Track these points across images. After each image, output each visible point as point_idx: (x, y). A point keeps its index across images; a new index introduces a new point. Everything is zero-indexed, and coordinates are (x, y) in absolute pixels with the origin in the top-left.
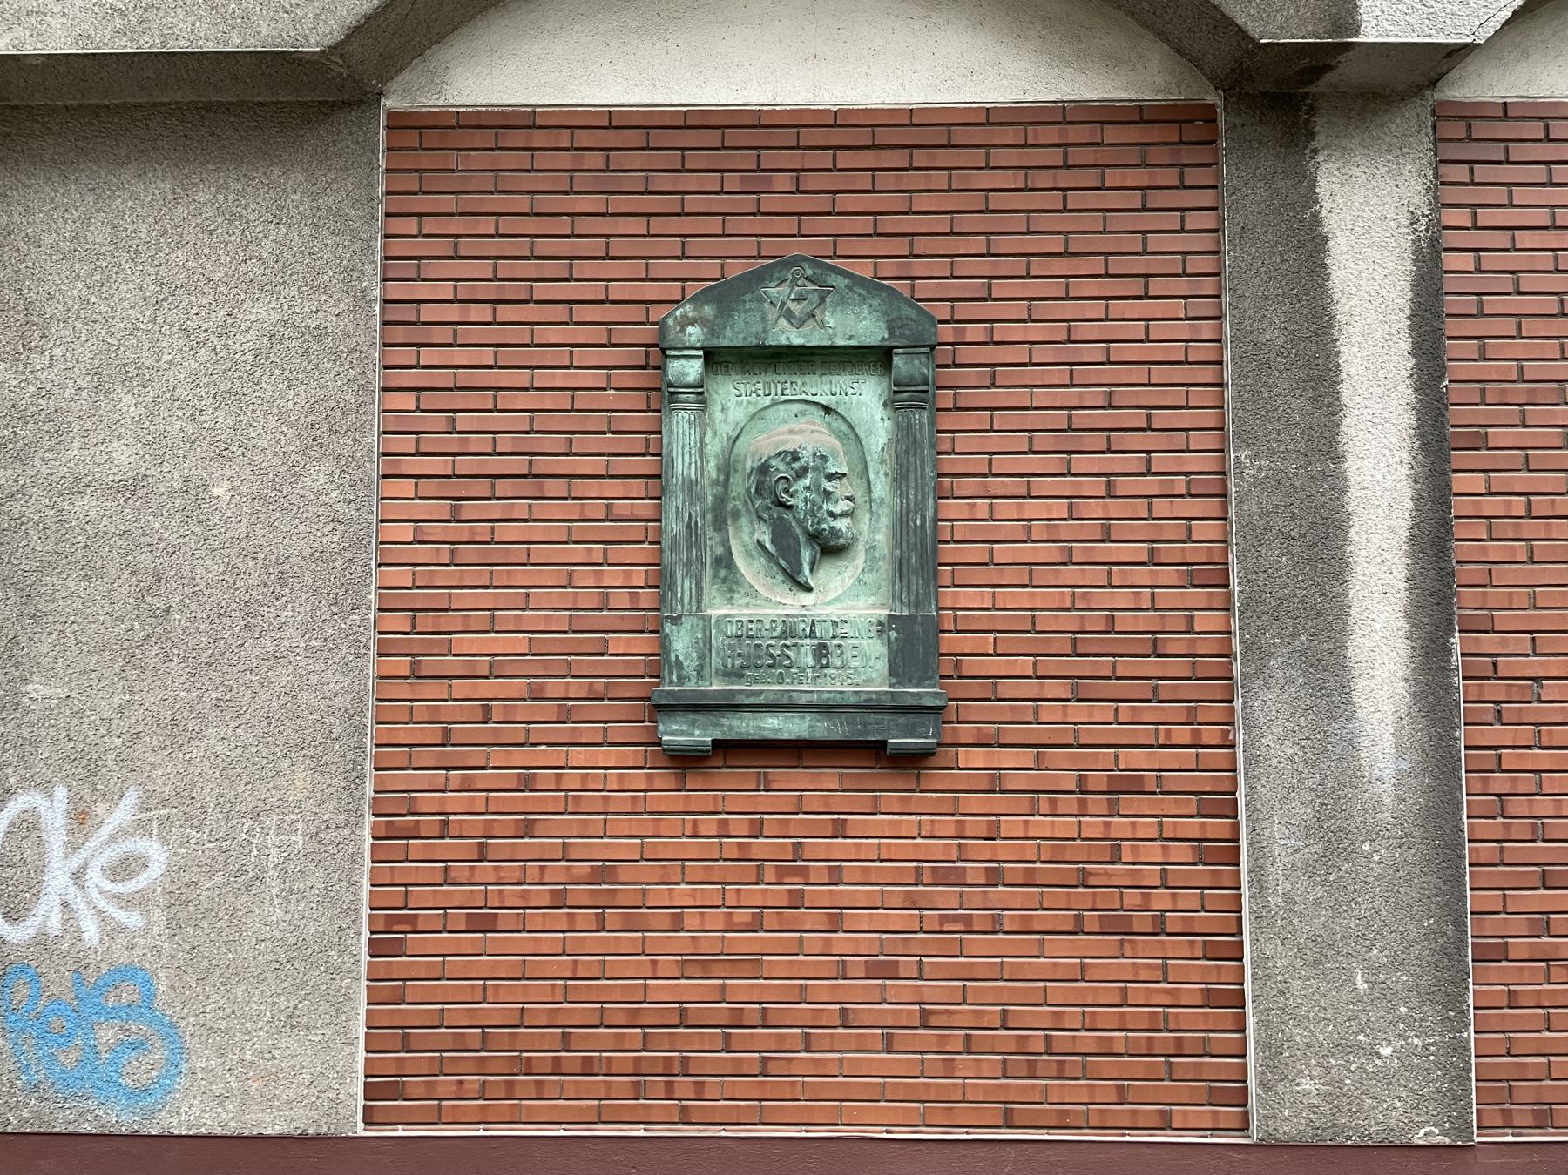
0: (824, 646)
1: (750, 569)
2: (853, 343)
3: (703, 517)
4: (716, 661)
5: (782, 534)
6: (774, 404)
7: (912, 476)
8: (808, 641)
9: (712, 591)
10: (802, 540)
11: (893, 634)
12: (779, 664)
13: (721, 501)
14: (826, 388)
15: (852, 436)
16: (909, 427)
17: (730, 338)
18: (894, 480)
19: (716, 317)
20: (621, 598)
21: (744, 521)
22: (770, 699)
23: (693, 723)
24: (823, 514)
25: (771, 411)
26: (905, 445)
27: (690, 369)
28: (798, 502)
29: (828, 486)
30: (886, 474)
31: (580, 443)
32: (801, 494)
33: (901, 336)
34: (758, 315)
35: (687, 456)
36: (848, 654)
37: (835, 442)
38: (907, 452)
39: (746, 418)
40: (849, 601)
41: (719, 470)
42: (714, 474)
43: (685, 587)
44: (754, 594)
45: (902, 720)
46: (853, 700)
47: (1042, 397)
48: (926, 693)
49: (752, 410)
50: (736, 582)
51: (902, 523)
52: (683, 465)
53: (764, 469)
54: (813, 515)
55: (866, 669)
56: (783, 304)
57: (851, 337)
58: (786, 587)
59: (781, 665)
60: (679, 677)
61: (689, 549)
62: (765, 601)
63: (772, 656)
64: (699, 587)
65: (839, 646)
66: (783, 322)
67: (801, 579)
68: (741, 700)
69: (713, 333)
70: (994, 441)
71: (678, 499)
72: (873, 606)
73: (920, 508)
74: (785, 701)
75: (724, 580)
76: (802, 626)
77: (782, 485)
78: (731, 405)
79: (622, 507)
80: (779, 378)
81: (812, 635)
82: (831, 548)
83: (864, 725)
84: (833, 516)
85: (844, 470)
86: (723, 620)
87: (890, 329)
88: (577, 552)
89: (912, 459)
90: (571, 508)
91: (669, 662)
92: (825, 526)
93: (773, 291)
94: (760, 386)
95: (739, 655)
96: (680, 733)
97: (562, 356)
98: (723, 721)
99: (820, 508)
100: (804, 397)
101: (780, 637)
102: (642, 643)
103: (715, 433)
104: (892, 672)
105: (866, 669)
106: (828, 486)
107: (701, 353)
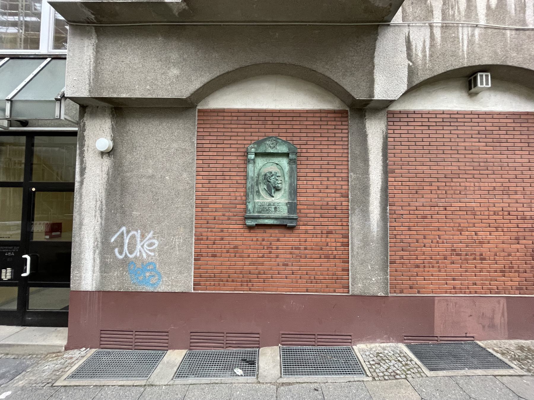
1: (263, 193)
4: (256, 210)
5: (268, 187)
9: (256, 197)
12: (268, 211)
13: (257, 181)
15: (282, 169)
20: (239, 198)
26: (291, 171)
27: (252, 156)
28: (272, 181)
32: (272, 180)
37: (279, 170)
40: (281, 199)
43: (251, 196)
44: (263, 198)
47: (316, 162)
48: (294, 216)
51: (290, 185)
52: (251, 174)
53: (265, 175)
55: (284, 212)
69: (256, 150)
70: (307, 170)
71: (250, 180)
73: (294, 183)
78: (260, 162)
79: (239, 181)
82: (277, 189)
86: (258, 202)
88: (231, 190)
90: (230, 182)
96: (249, 223)
102: (243, 206)
104: (288, 212)
105: (284, 212)
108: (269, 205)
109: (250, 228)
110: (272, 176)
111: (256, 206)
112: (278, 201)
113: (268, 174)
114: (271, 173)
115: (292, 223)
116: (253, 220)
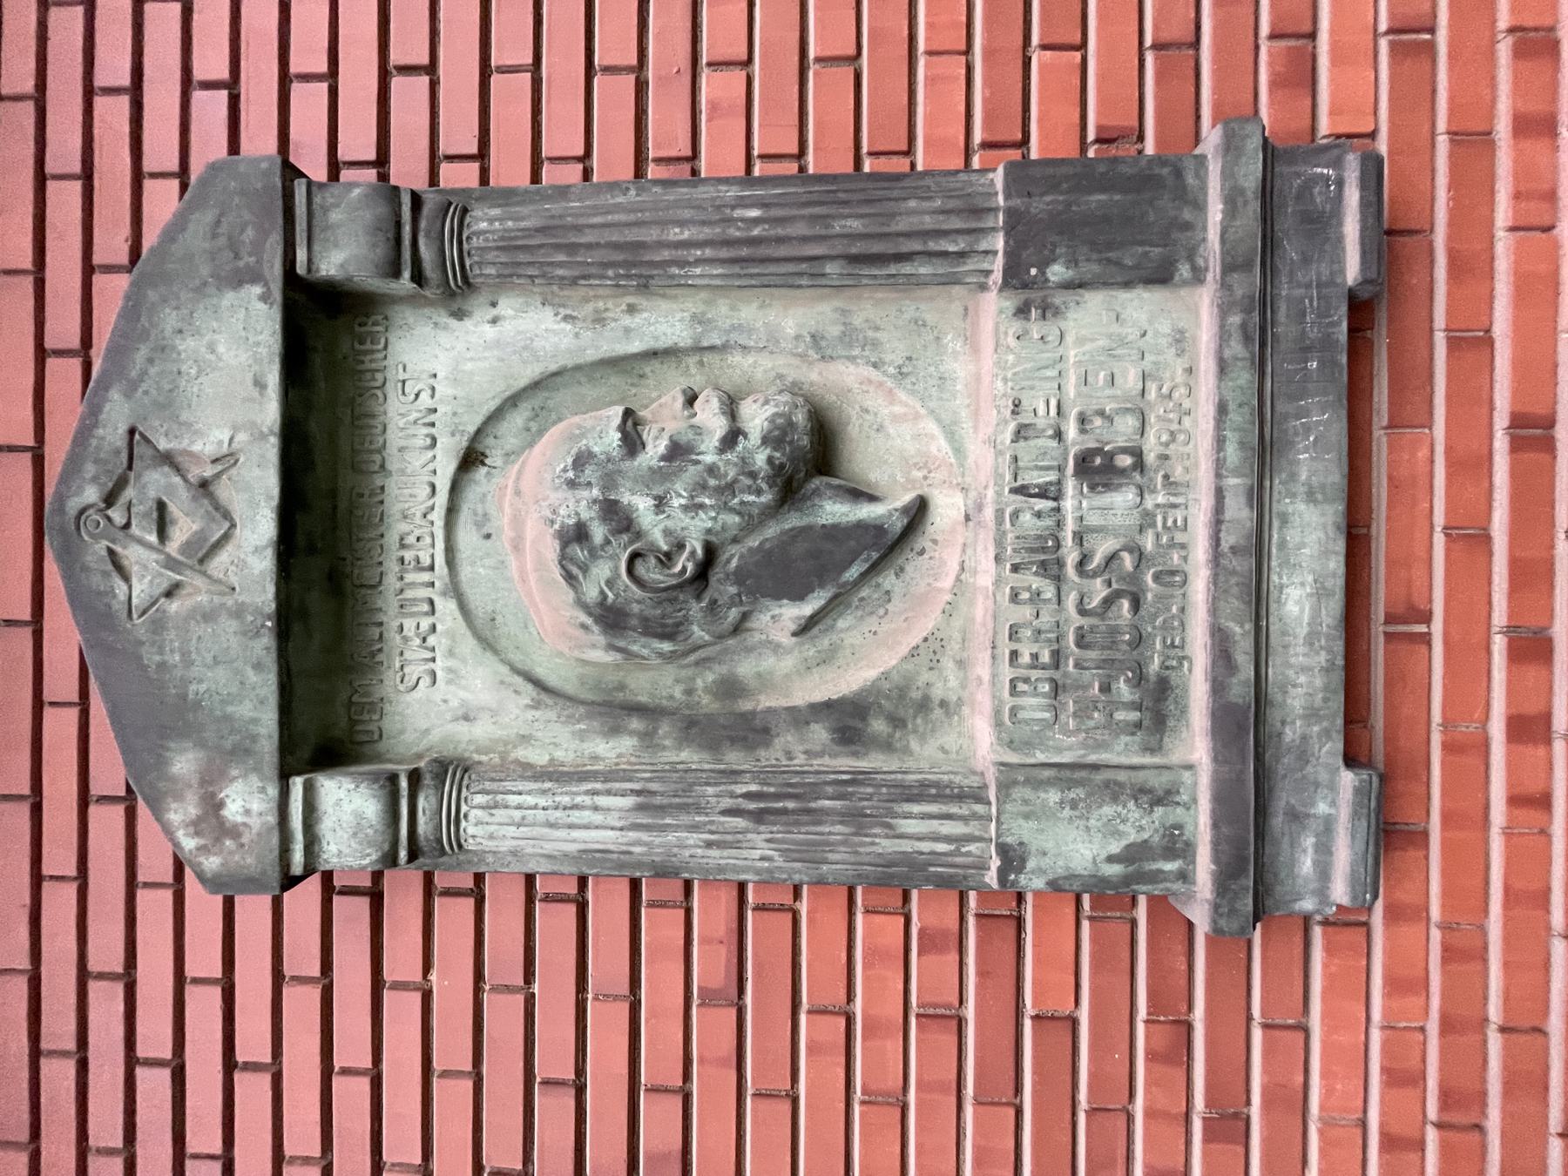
0: (1084, 465)
1: (865, 656)
2: (273, 378)
3: (733, 775)
4: (1123, 752)
5: (780, 575)
6: (455, 591)
7: (632, 235)
8: (1068, 504)
9: (926, 755)
10: (793, 521)
11: (1057, 272)
12: (1135, 581)
13: (694, 728)
14: (416, 461)
15: (538, 394)
16: (508, 245)
17: (257, 707)
18: (644, 287)
19: (201, 744)
20: (929, 976)
21: (746, 668)
22: (1234, 604)
23: (1296, 817)
24: (728, 465)
25: (479, 600)
26: (562, 259)
27: (347, 808)
28: (695, 530)
29: (655, 449)
31: (554, 1060)
32: (677, 521)
34: (198, 629)
35: (576, 816)
37: (555, 432)
38: (572, 248)
40: (952, 399)
41: (614, 731)
43: (918, 831)
44: (931, 649)
45: (1291, 251)
46: (1244, 377)
49: (468, 644)
50: (902, 692)
51: (757, 262)
52: (599, 826)
53: (610, 618)
54: (730, 488)
57: (260, 384)
58: (915, 566)
59: (1135, 577)
61: (817, 816)
63: (1108, 602)
65: (1083, 420)
67: (898, 524)
69: (242, 752)
71: (685, 843)
73: (721, 213)
74: (1245, 565)
75: (897, 722)
76: (1026, 518)
77: (649, 570)
78: (456, 697)
79: (710, 966)
80: (391, 582)
81: (1050, 492)
82: (814, 452)
83: (1305, 351)
86: (1008, 727)
87: (239, 279)
89: (588, 237)
90: (711, 1089)
91: (1127, 880)
93: (141, 589)
94: (409, 625)
95: (1106, 688)
97: (351, 1095)
98: (1290, 735)
100: (438, 517)
101: (1058, 579)
103: (525, 739)
106: (655, 449)
108: (1051, 569)
109: (1390, 835)
110: (617, 517)
111: (1066, 747)
113: (591, 593)
114: (579, 534)
115: (1322, 225)
116: (1283, 799)
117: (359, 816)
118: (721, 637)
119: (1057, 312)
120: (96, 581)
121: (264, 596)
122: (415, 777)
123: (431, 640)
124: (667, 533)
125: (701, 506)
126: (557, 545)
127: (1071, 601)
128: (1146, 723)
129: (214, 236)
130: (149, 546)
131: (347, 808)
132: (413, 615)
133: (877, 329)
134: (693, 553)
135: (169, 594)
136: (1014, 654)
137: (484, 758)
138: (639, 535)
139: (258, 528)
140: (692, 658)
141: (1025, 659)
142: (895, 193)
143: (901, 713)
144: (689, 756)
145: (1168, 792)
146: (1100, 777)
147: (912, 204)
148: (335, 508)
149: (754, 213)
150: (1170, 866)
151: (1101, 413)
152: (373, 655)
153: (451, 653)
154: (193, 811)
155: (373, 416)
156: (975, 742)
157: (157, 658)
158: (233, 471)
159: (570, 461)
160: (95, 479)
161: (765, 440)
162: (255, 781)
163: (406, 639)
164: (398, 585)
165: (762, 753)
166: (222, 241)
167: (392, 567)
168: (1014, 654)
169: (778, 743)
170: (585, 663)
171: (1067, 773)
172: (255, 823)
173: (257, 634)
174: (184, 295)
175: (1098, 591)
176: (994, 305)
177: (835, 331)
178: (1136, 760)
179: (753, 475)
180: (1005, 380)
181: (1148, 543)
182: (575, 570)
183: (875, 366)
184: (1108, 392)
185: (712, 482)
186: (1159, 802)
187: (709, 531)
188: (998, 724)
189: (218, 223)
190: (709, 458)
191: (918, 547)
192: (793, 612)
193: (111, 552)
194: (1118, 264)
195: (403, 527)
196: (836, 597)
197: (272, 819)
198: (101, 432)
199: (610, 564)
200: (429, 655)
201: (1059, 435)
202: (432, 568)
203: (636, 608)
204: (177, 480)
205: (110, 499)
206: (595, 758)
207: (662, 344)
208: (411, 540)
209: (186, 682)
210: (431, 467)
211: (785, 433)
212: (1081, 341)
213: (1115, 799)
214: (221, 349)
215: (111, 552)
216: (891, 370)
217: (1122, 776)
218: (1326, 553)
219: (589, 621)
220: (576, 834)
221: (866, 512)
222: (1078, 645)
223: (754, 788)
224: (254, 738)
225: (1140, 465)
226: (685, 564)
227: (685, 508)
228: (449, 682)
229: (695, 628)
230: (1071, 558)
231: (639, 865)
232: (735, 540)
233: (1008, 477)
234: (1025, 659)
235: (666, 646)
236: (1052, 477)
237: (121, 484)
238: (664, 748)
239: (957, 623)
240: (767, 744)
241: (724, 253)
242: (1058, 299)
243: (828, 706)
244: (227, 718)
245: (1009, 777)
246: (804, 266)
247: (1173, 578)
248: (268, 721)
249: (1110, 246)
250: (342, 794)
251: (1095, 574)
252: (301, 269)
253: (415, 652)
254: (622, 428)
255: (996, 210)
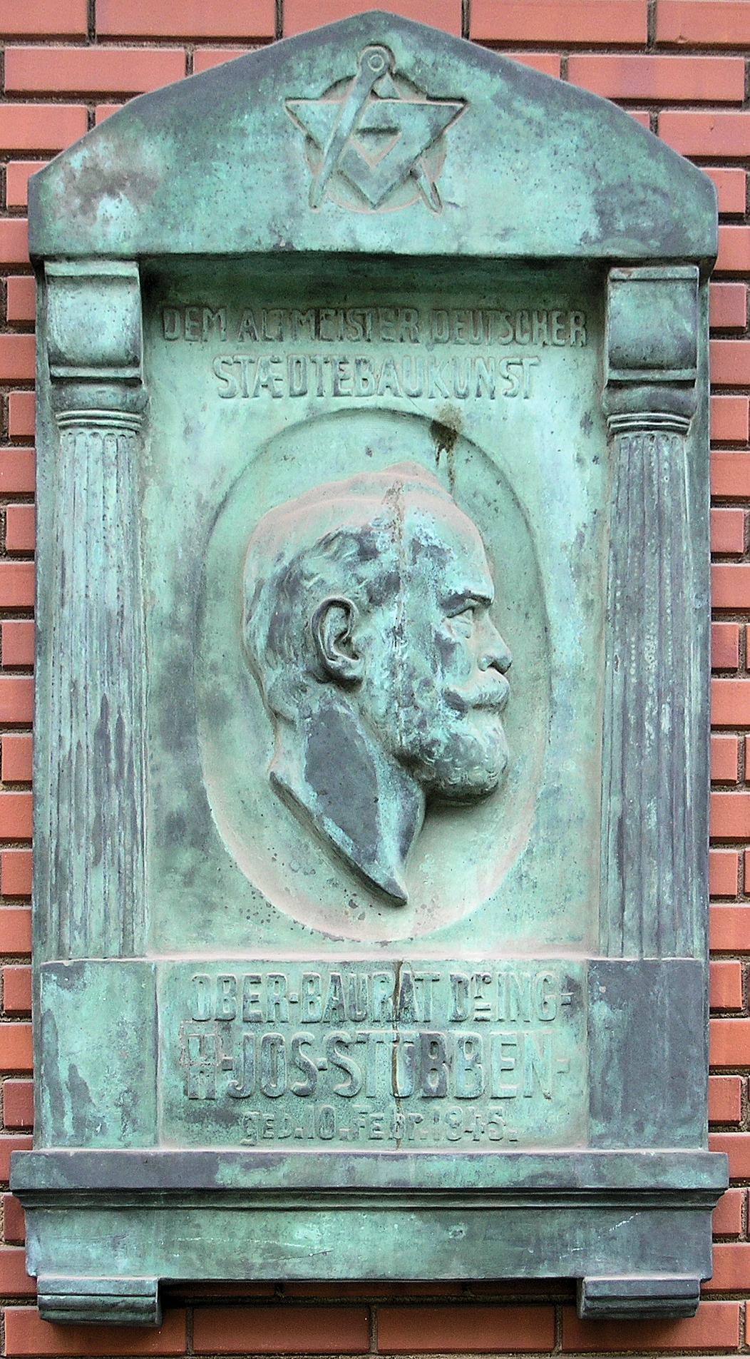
4: (169, 1082)
5: (331, 758)
6: (314, 418)
10: (383, 769)
11: (601, 1011)
13: (180, 672)
19: (170, 174)
21: (238, 726)
25: (305, 442)
28: (372, 668)
30: (588, 604)
33: (631, 232)
34: (277, 169)
36: (495, 1061)
39: (239, 453)
41: (178, 590)
42: (165, 602)
43: (92, 890)
44: (261, 913)
49: (261, 432)
50: (217, 882)
53: (289, 584)
54: (411, 702)
56: (339, 141)
57: (505, 234)
60: (79, 1123)
62: (279, 934)
63: (305, 1069)
64: (128, 895)
66: (337, 196)
67: (377, 874)
68: (228, 1176)
72: (552, 943)
74: (338, 1179)
78: (209, 420)
80: (323, 349)
82: (449, 798)
84: (457, 704)
85: (484, 588)
92: (437, 732)
93: (315, 111)
94: (279, 370)
99: (427, 683)
100: (388, 400)
103: (168, 494)
104: (598, 1108)
107: (132, 270)
108: (337, 1013)
112: (470, 955)
113: (310, 565)
114: (367, 553)
117: (100, 328)
118: (269, 699)
119: (569, 1016)
120: (324, 64)
121: (309, 239)
122: (133, 383)
123: (265, 393)
124: (369, 641)
125: (393, 674)
126: (357, 530)
127: (307, 1034)
128: (195, 1103)
129: (645, 187)
130: (355, 122)
131: (107, 317)
132: (290, 375)
133: (564, 853)
134: (350, 666)
135: (309, 139)
136: (256, 981)
137: (148, 449)
138: (366, 612)
139: (372, 233)
140: (247, 671)
141: (253, 991)
142: (680, 862)
143: (197, 881)
144: (151, 670)
145: (134, 1122)
146: (146, 1057)
147: (669, 877)
148: (397, 290)
149: (666, 725)
150: (68, 1122)
151: (476, 1060)
152: (251, 331)
153: (252, 414)
154: (108, 166)
155: (486, 332)
156: (173, 948)
157: (250, 129)
158: (425, 208)
159: (436, 543)
160: (418, 62)
161: (455, 737)
162: (136, 229)
163: (266, 367)
164: (320, 359)
165: (158, 741)
166: (641, 195)
167: (338, 349)
168: (256, 981)
169: (167, 758)
170: (243, 557)
171: (150, 1029)
172: (95, 230)
173: (272, 231)
174: (589, 157)
175: (316, 1059)
176: (575, 961)
177: (563, 812)
178: (160, 1095)
179: (422, 724)
180: (508, 969)
181: (360, 1104)
182: (335, 547)
183: (529, 852)
184: (496, 1067)
185: (415, 685)
186: (126, 1113)
187: (370, 683)
188: (193, 966)
189: (655, 190)
190: (438, 682)
191: (357, 900)
192: (295, 776)
193: (350, 78)
194: (607, 1067)
195: (377, 362)
196: (308, 813)
197: (100, 246)
198: (463, 67)
199: (340, 584)
200: (250, 392)
201: (457, 1021)
202: (337, 394)
203: (298, 609)
204: (417, 150)
205: (400, 76)
206: (149, 568)
207: (554, 634)
208: (365, 372)
209: (227, 156)
210: (438, 394)
211: (462, 757)
212: (541, 1041)
213: (128, 1073)
214: (539, 194)
215: (350, 78)
216: (525, 868)
217: (148, 1078)
218: (348, 1261)
219: (286, 562)
220: (81, 550)
221: (389, 845)
222: (266, 1039)
223: (127, 730)
224: (174, 228)
225: (428, 1098)
226: (339, 660)
227: (392, 658)
228: (223, 412)
229: (279, 671)
230: (345, 1034)
231: (48, 615)
232: (362, 711)
233: (419, 974)
234: (253, 991)
235: (261, 642)
236: (419, 1015)
237: (416, 88)
238: (160, 641)
239: (285, 936)
240: (167, 746)
241: (632, 696)
242: (580, 1016)
243: (204, 808)
244: (195, 200)
245: (144, 974)
246: (618, 776)
247: (326, 1130)
248: (185, 241)
249: (624, 1060)
250: (122, 312)
251: (330, 1055)
252: (615, 272)
253: (253, 376)
254: (468, 595)
255: (659, 954)
